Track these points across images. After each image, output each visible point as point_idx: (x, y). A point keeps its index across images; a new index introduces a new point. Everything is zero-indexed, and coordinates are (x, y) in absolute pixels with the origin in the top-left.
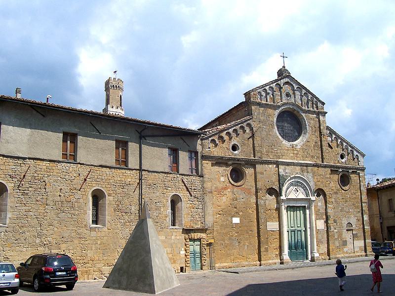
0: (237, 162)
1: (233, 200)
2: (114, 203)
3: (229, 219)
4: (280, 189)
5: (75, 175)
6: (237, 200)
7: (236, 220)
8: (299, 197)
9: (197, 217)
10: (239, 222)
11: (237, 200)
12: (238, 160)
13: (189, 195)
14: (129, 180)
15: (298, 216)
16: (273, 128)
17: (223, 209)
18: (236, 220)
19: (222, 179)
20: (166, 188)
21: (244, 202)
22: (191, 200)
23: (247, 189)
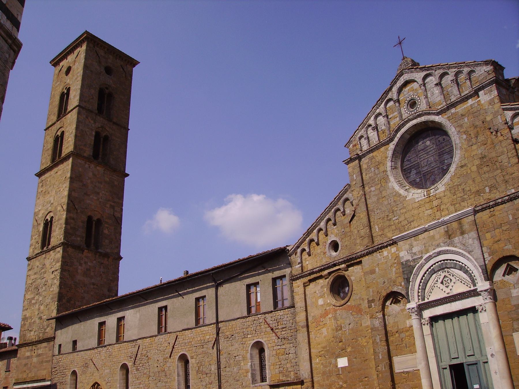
0: (335, 268)
1: (337, 330)
2: (195, 365)
3: (333, 361)
4: (407, 289)
5: (166, 345)
6: (341, 329)
7: (343, 362)
8: (455, 291)
9: (288, 365)
10: (348, 365)
11: (341, 329)
12: (335, 265)
13: (274, 338)
14: (208, 337)
15: (465, 331)
16: (386, 179)
17: (324, 348)
18: (343, 362)
19: (321, 302)
20: (245, 336)
21: (352, 329)
22: (279, 344)
23: (355, 306)
